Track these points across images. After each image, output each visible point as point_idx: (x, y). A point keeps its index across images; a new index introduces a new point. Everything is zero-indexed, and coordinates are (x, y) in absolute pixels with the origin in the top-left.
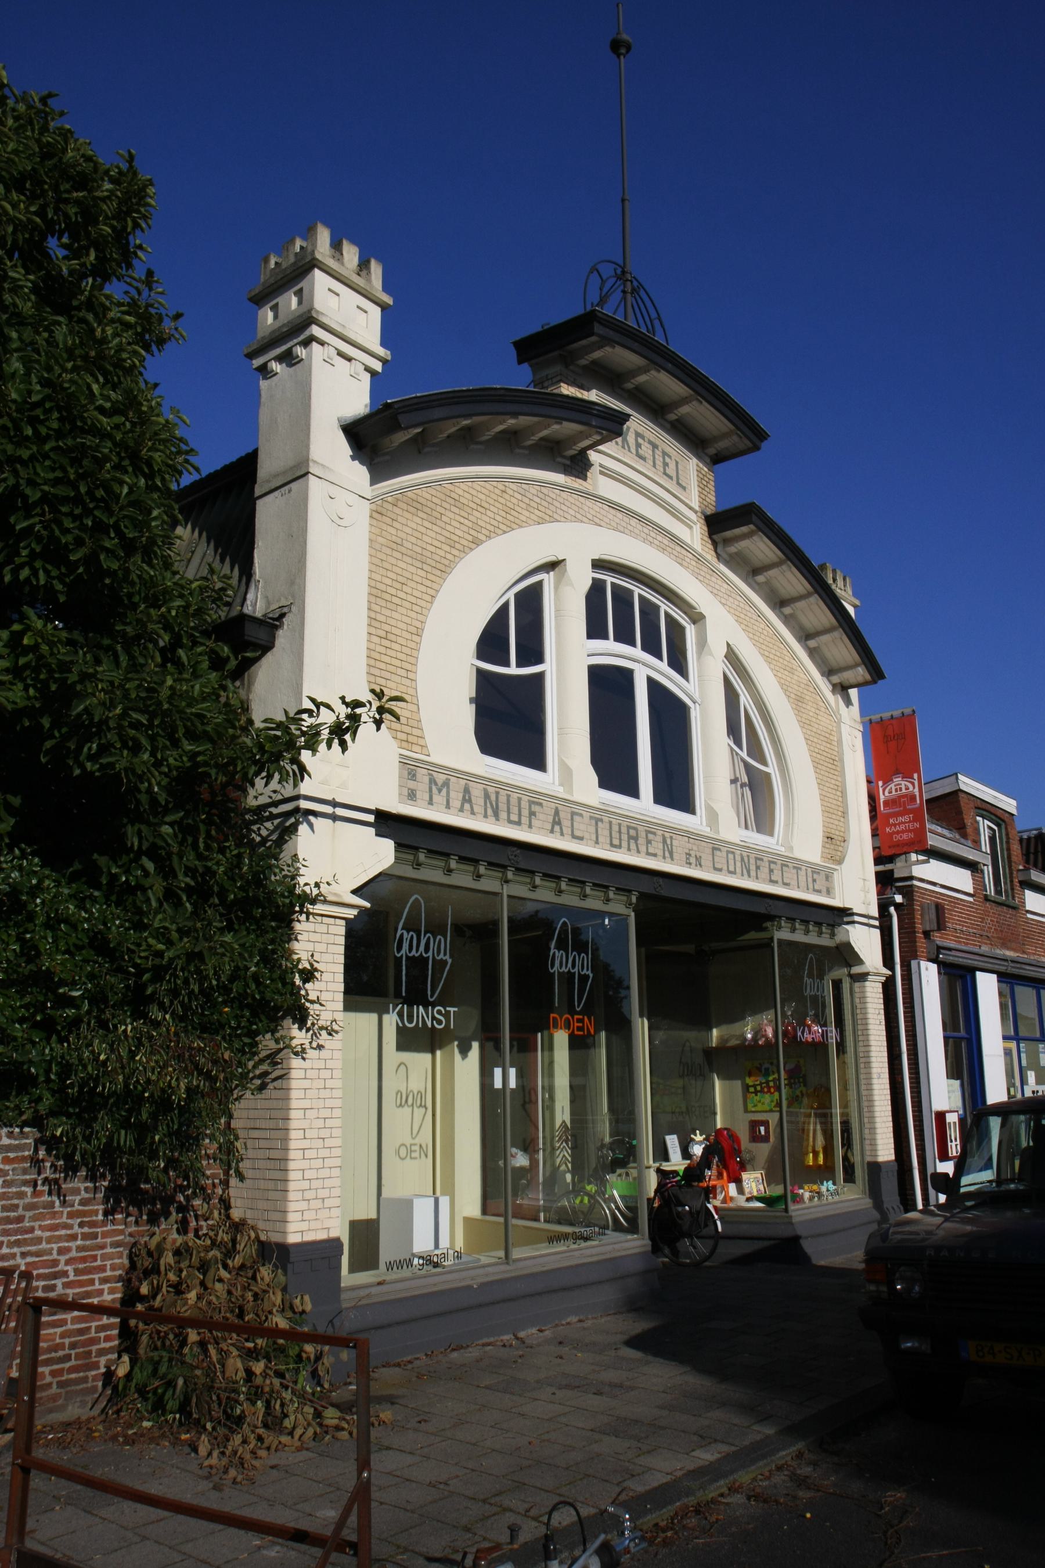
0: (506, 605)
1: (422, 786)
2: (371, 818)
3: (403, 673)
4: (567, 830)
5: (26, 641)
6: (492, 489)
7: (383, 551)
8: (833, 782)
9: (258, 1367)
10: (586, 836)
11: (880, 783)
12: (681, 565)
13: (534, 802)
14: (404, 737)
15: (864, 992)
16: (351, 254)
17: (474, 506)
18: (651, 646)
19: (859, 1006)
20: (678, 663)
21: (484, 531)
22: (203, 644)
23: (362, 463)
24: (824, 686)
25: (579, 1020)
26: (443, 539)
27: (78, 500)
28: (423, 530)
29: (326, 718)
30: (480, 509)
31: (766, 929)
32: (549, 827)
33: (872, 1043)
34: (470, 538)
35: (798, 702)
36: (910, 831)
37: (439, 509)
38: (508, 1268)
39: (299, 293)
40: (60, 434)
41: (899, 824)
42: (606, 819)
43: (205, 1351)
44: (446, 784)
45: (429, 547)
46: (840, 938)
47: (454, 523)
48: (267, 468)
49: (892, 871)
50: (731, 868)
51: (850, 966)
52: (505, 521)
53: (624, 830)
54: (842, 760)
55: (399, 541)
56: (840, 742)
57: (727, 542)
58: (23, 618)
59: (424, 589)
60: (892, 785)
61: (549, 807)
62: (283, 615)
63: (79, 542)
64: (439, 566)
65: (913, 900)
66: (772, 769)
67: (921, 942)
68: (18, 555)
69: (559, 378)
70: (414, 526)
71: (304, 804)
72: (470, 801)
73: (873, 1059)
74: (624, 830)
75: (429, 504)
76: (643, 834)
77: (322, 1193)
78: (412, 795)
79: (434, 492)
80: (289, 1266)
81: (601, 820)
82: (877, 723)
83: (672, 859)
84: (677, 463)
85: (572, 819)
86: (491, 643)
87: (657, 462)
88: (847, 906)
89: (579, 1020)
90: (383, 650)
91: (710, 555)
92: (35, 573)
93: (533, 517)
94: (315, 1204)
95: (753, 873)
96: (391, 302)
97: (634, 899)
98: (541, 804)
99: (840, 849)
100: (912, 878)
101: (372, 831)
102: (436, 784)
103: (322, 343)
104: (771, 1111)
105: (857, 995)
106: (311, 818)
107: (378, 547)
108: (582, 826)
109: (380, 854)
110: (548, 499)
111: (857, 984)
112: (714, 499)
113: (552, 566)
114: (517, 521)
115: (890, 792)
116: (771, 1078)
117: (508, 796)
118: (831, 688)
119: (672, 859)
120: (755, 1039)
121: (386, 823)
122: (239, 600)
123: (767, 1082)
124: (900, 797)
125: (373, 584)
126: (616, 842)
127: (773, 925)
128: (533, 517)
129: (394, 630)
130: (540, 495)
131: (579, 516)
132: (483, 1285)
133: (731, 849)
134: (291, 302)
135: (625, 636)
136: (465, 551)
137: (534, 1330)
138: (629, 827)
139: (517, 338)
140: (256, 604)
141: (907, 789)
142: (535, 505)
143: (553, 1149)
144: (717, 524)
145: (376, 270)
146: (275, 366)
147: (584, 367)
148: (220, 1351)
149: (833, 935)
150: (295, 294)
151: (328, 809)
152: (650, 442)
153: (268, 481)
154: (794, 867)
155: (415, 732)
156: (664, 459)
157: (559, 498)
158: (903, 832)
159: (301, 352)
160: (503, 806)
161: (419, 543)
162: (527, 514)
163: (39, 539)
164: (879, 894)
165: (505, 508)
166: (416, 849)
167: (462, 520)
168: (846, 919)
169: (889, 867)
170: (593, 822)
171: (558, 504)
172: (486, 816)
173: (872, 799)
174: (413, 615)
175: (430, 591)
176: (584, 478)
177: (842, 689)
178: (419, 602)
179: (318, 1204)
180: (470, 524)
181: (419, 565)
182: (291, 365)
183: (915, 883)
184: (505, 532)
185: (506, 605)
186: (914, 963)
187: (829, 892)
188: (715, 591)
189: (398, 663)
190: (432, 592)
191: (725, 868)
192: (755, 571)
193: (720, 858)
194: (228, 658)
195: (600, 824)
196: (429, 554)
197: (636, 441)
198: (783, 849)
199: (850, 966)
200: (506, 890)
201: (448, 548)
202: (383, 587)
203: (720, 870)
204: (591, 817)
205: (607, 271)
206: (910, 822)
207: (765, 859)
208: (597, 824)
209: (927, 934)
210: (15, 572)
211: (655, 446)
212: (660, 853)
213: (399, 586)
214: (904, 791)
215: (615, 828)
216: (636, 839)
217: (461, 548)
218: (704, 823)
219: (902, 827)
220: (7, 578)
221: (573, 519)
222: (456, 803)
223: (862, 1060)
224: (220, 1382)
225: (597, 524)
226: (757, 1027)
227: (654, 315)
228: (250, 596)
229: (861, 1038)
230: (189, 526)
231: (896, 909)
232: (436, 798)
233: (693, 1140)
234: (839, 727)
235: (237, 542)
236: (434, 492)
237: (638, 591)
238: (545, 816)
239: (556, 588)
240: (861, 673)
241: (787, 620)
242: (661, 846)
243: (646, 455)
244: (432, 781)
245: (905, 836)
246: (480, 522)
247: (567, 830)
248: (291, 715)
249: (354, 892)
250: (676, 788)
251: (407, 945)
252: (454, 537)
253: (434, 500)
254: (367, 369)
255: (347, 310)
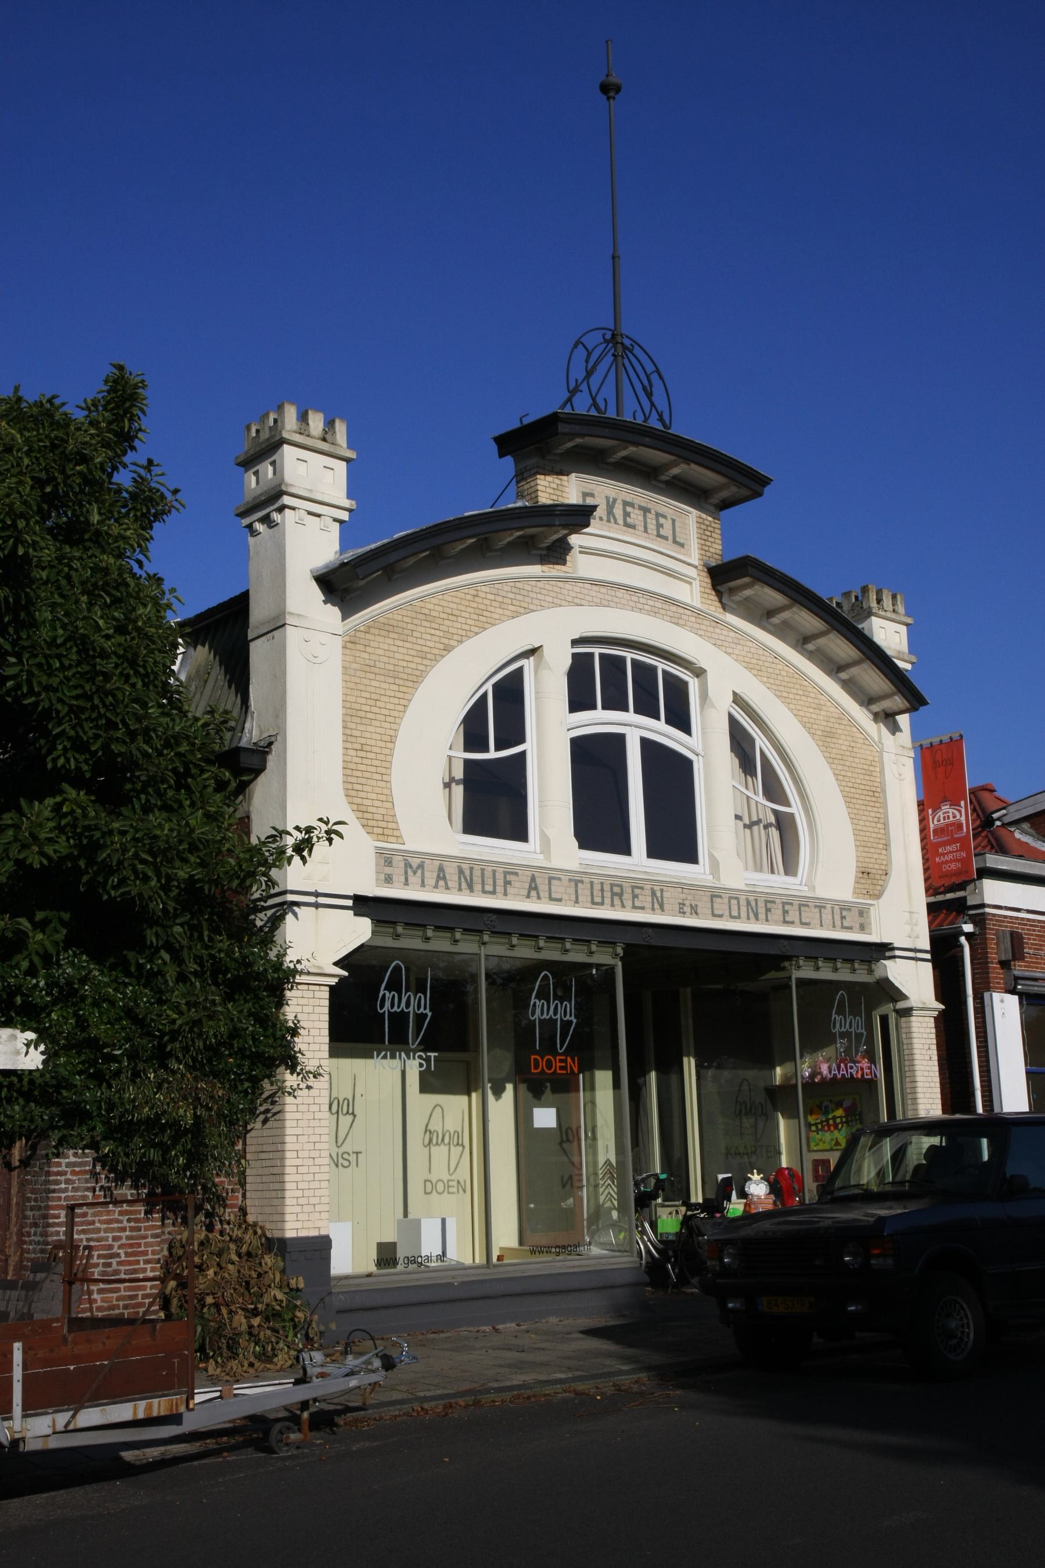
0: (484, 696)
1: (398, 871)
2: (350, 903)
3: (379, 777)
4: (544, 894)
5: (65, 809)
6: (463, 596)
7: (354, 676)
8: (873, 814)
9: (256, 1321)
10: (565, 897)
11: (930, 811)
12: (677, 624)
13: (509, 873)
14: (380, 831)
15: (910, 1027)
16: (316, 422)
17: (445, 616)
18: (647, 707)
19: (905, 1041)
20: (680, 719)
21: (455, 637)
22: (208, 771)
23: (334, 605)
24: (861, 716)
25: (561, 1061)
26: (414, 653)
27: (94, 708)
28: (395, 649)
29: (290, 841)
30: (451, 617)
31: (784, 969)
32: (525, 893)
33: (918, 1079)
34: (442, 646)
35: (825, 738)
36: (956, 860)
37: (410, 626)
38: (488, 1271)
39: (273, 463)
40: (79, 663)
41: (947, 853)
42: (587, 880)
43: (219, 1311)
44: (421, 866)
45: (401, 663)
46: (878, 973)
47: (425, 636)
48: (258, 613)
49: (964, 899)
50: (735, 913)
51: (895, 1001)
52: (477, 623)
53: (607, 888)
54: (884, 791)
55: (372, 663)
56: (882, 772)
57: (732, 591)
58: (61, 792)
59: (396, 701)
60: (941, 813)
61: (525, 877)
62: (271, 744)
63: (97, 737)
64: (411, 678)
65: (985, 928)
66: (796, 808)
67: (996, 972)
68: (55, 749)
69: (535, 470)
70: (386, 647)
71: (290, 898)
72: (444, 878)
73: (919, 1095)
74: (607, 888)
75: (401, 624)
76: (630, 890)
77: (313, 1201)
78: (389, 880)
79: (405, 613)
80: (287, 1255)
81: (582, 882)
82: (927, 748)
83: (662, 909)
84: (674, 521)
85: (550, 883)
86: (473, 732)
87: (650, 526)
88: (885, 940)
89: (561, 1061)
90: (359, 760)
91: (712, 606)
92: (68, 760)
93: (507, 613)
94: (306, 1208)
95: (762, 916)
96: (354, 457)
97: (620, 950)
98: (516, 874)
99: (881, 882)
100: (983, 906)
101: (351, 912)
102: (411, 867)
103: (293, 509)
104: (831, 1150)
105: (904, 1030)
106: (295, 908)
107: (352, 672)
108: (558, 889)
109: (359, 931)
110: (523, 592)
111: (903, 1019)
112: (720, 547)
113: (532, 652)
114: (489, 620)
115: (939, 821)
116: (830, 1116)
117: (483, 870)
118: (871, 717)
119: (662, 909)
120: (813, 1075)
121: (362, 904)
122: (239, 728)
123: (827, 1120)
124: (948, 825)
125: (348, 705)
126: (598, 899)
127: (791, 965)
128: (507, 613)
129: (369, 742)
130: (514, 590)
131: (556, 601)
132: (463, 1283)
133: (734, 896)
134: (267, 470)
135: (615, 702)
136: (436, 659)
137: (513, 1325)
138: (612, 885)
139: (497, 435)
140: (253, 733)
141: (954, 817)
142: (509, 602)
143: (596, 1186)
144: (722, 577)
145: (341, 429)
146: (259, 527)
147: (562, 454)
148: (230, 1312)
149: (871, 971)
150: (271, 464)
151: (311, 899)
152: (641, 508)
153: (257, 627)
154: (816, 906)
155: (391, 825)
156: (657, 520)
157: (535, 589)
158: (951, 861)
159: (276, 516)
160: (477, 879)
161: (391, 661)
162: (501, 611)
163: (69, 739)
164: (930, 924)
165: (477, 611)
166: (395, 923)
167: (433, 632)
168: (887, 954)
169: (960, 894)
170: (573, 884)
171: (534, 595)
172: (460, 889)
173: (923, 829)
174: (387, 725)
175: (402, 702)
176: (563, 562)
177: (888, 718)
178: (393, 713)
179: (310, 1208)
180: (441, 634)
181: (391, 680)
182: (271, 527)
183: (988, 910)
184: (477, 634)
185: (484, 696)
186: (986, 995)
187: (862, 928)
188: (720, 643)
189: (373, 769)
190: (405, 702)
191: (727, 913)
192: (770, 613)
193: (721, 906)
194: (229, 780)
195: (580, 885)
196: (401, 669)
197: (624, 510)
198: (806, 888)
199: (896, 1001)
200: (483, 951)
201: (419, 660)
202: (358, 707)
203: (721, 916)
204: (570, 880)
205: (594, 340)
206: (957, 851)
207: (777, 901)
208: (576, 885)
209: (1005, 965)
210: (55, 760)
211: (646, 510)
212: (648, 905)
213: (372, 703)
214: (951, 819)
215: (597, 887)
216: (620, 895)
217: (433, 657)
218: (708, 872)
219: (951, 857)
220: (49, 766)
221: (551, 605)
222: (431, 881)
223: (909, 1096)
224: (228, 1331)
225: (577, 605)
226: (818, 1065)
227: (650, 368)
228: (247, 725)
229: (908, 1074)
230: (207, 646)
231: (967, 939)
232: (411, 879)
233: (750, 1179)
234: (881, 757)
235: (237, 670)
236: (405, 613)
237: (629, 655)
238: (520, 885)
239: (536, 672)
240: (898, 701)
241: (811, 656)
242: (649, 899)
243: (636, 522)
244: (408, 865)
245: (953, 866)
246: (451, 630)
247: (544, 894)
248: (263, 839)
249: (336, 964)
250: (675, 838)
251: (389, 1002)
252: (425, 649)
253: (406, 619)
254: (335, 520)
255: (316, 476)
